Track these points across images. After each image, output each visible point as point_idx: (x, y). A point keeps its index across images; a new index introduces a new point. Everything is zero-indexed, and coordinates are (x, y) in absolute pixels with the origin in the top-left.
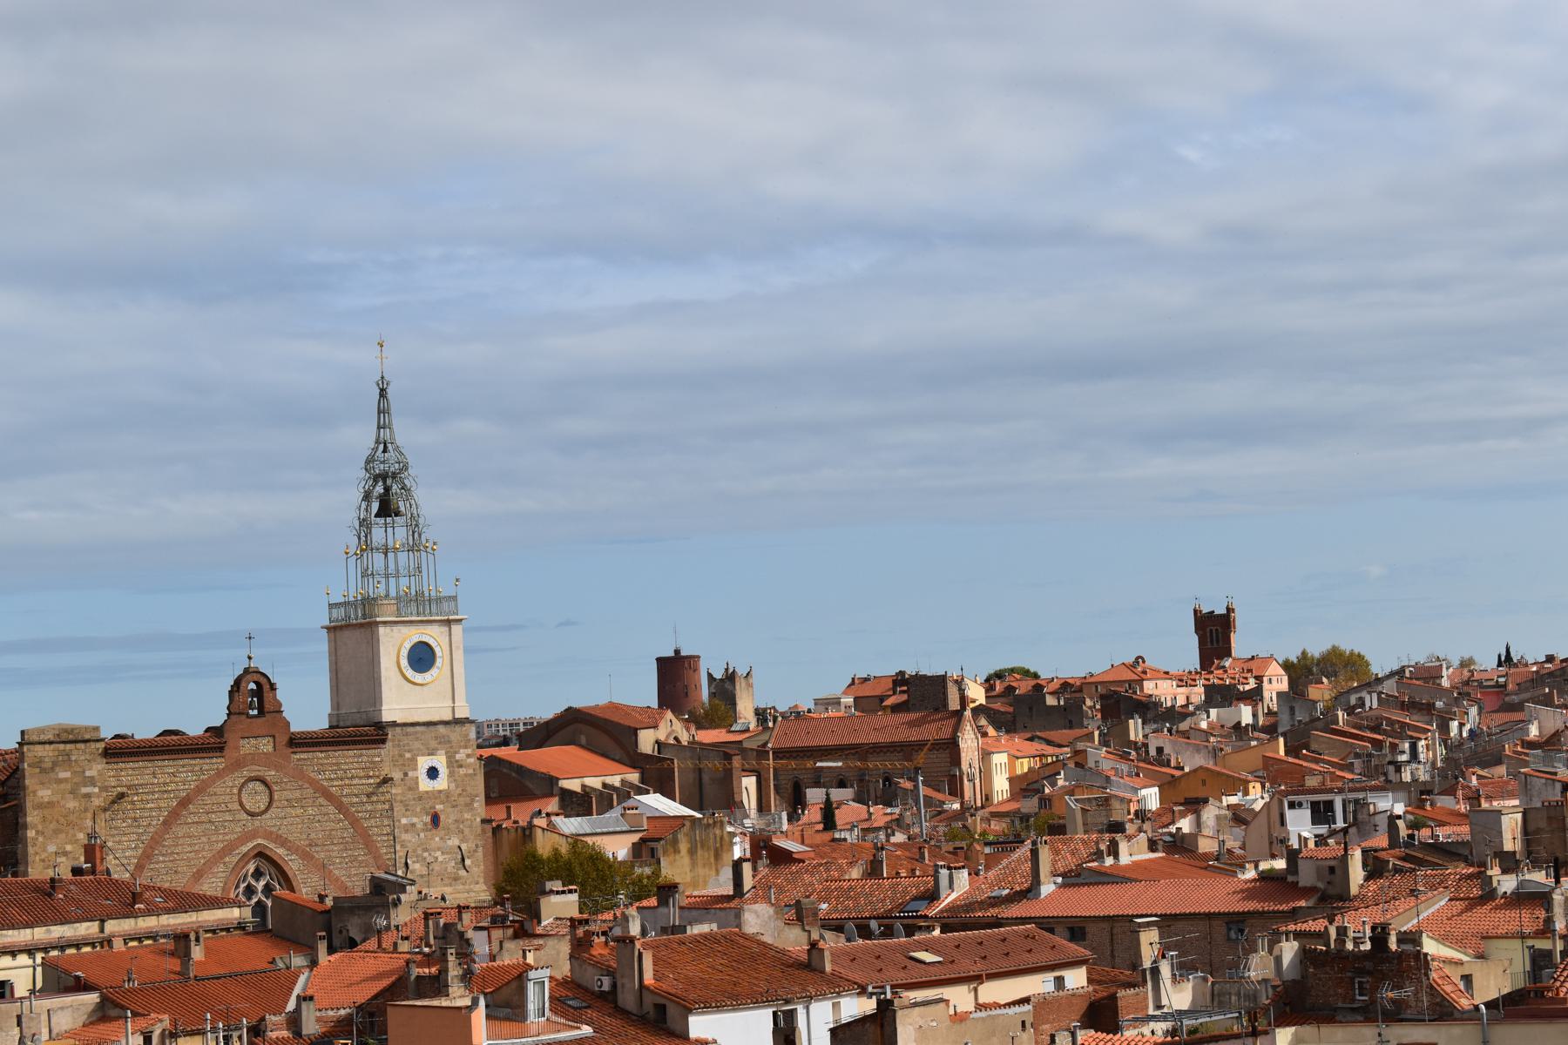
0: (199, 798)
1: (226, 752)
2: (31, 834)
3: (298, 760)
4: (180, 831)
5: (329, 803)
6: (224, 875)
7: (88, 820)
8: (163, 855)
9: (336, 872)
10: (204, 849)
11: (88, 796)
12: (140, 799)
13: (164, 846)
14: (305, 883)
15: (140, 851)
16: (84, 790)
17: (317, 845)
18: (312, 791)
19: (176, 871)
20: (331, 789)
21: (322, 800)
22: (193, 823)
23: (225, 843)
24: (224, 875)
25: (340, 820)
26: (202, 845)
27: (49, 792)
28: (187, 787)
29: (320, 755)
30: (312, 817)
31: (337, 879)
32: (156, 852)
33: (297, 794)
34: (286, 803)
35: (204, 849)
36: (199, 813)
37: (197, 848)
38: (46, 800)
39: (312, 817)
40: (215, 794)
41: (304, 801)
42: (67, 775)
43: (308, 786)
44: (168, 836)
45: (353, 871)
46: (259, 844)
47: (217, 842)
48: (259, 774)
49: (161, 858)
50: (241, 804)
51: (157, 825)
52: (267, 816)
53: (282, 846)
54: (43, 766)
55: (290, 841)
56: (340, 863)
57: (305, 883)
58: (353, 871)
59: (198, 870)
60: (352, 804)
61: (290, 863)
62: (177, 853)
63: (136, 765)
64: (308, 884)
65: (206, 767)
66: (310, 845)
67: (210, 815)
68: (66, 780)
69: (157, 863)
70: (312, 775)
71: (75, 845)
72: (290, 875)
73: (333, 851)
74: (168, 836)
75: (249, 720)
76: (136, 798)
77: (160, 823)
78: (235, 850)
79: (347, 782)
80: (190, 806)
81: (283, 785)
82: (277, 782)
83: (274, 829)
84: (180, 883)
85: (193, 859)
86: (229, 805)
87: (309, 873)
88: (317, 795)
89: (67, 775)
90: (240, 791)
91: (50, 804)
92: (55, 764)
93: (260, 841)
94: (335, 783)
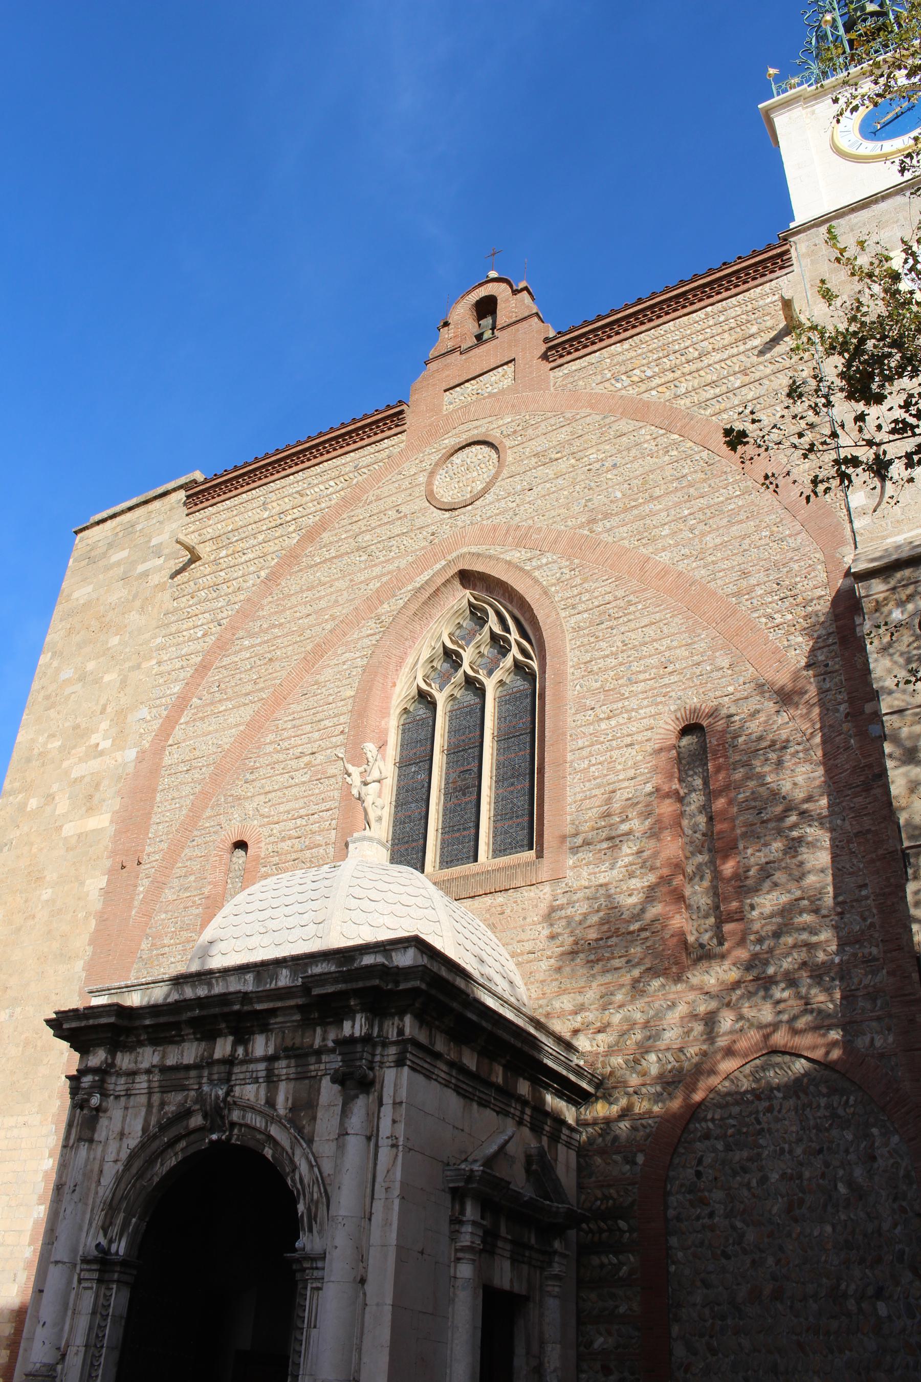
0: (344, 516)
1: (410, 418)
2: (44, 659)
3: (566, 376)
4: (290, 584)
5: (641, 424)
6: (367, 642)
7: (134, 613)
8: (251, 636)
9: (664, 557)
10: (336, 601)
11: (145, 574)
12: (230, 552)
13: (259, 618)
14: (573, 607)
15: (211, 640)
16: (141, 568)
17: (607, 516)
18: (598, 418)
19: (271, 660)
20: (646, 395)
21: (624, 425)
22: (324, 562)
23: (384, 579)
24: (367, 642)
25: (675, 443)
26: (334, 597)
27: (90, 588)
28: (323, 505)
29: (618, 348)
30: (597, 465)
31: (665, 572)
32: (241, 633)
33: (563, 435)
34: (534, 460)
35: (336, 601)
36: (341, 539)
37: (323, 604)
38: (82, 602)
39: (597, 465)
40: (378, 499)
41: (577, 442)
42: (124, 554)
43: (588, 411)
44: (270, 599)
45: (711, 540)
46: (463, 556)
47: (367, 582)
48: (476, 432)
49: (247, 642)
50: (430, 497)
51: (254, 585)
52: (489, 497)
53: (517, 545)
54: (93, 554)
55: (539, 530)
56: (674, 533)
57: (573, 607)
58: (711, 540)
59: (318, 645)
60: (704, 404)
61: (536, 574)
62: (281, 624)
63: (236, 501)
64: (581, 607)
65: (367, 460)
66: (594, 521)
67: (360, 539)
68: (118, 563)
69: (236, 653)
70: (599, 389)
71: (101, 660)
72: (531, 596)
73: (652, 514)
74: (270, 599)
75: (464, 357)
76: (223, 553)
77: (258, 581)
78: (404, 585)
79: (687, 368)
80: (324, 535)
81: (530, 431)
82: (515, 432)
83: (501, 519)
84: (275, 679)
85: (310, 627)
86: (401, 508)
87: (585, 580)
88: (607, 421)
89: (124, 554)
90: (432, 474)
91: (87, 605)
92: (110, 545)
93: (465, 550)
94: (657, 381)
